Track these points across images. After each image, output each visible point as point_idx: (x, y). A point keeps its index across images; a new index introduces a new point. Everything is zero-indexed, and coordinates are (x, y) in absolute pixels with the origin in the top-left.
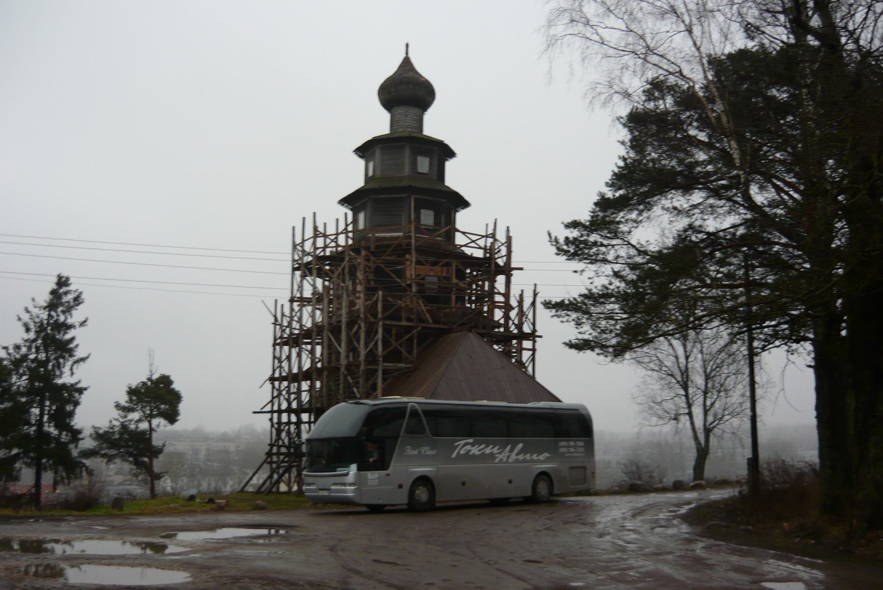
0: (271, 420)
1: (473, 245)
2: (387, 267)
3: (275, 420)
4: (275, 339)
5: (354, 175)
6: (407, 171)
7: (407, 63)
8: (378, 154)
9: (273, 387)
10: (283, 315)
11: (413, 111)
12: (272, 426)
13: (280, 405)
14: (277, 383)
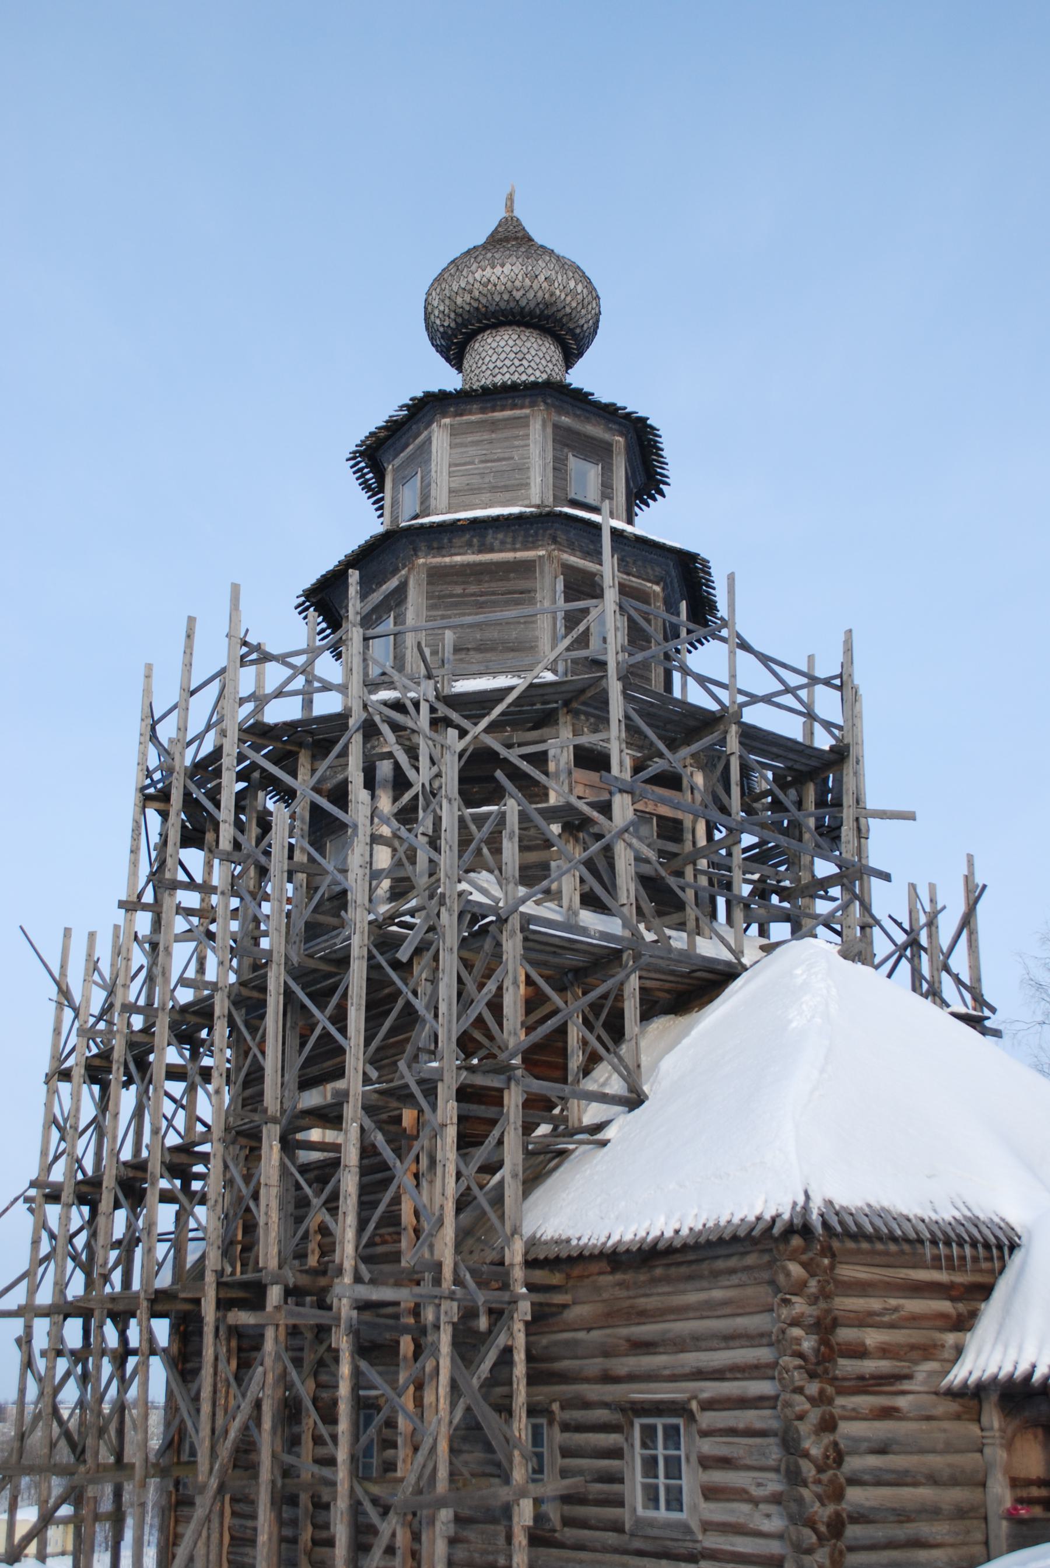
0: (25, 1342)
1: (788, 700)
2: (509, 746)
3: (40, 1341)
4: (58, 1057)
9: (42, 1224)
10: (93, 966)
12: (28, 1364)
13: (61, 1286)
14: (53, 1212)
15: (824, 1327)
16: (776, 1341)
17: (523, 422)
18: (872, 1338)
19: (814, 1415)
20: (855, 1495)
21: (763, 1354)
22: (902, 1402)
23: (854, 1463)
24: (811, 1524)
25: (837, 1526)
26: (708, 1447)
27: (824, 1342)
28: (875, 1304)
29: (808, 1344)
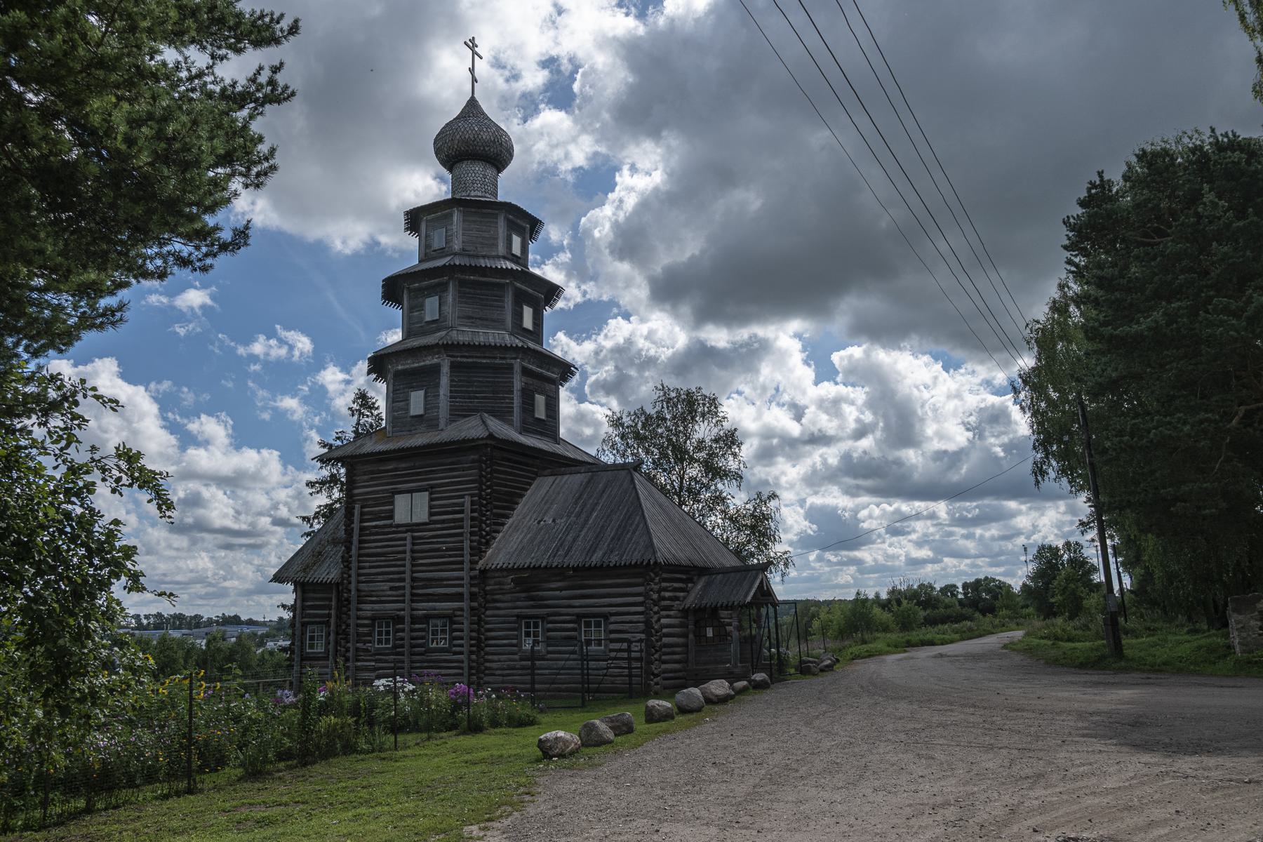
6: (501, 249)
7: (472, 104)
8: (456, 216)
11: (490, 172)
16: (646, 595)
17: (496, 217)
18: (667, 594)
19: (656, 617)
20: (665, 640)
22: (672, 613)
23: (665, 630)
26: (612, 627)
29: (655, 596)
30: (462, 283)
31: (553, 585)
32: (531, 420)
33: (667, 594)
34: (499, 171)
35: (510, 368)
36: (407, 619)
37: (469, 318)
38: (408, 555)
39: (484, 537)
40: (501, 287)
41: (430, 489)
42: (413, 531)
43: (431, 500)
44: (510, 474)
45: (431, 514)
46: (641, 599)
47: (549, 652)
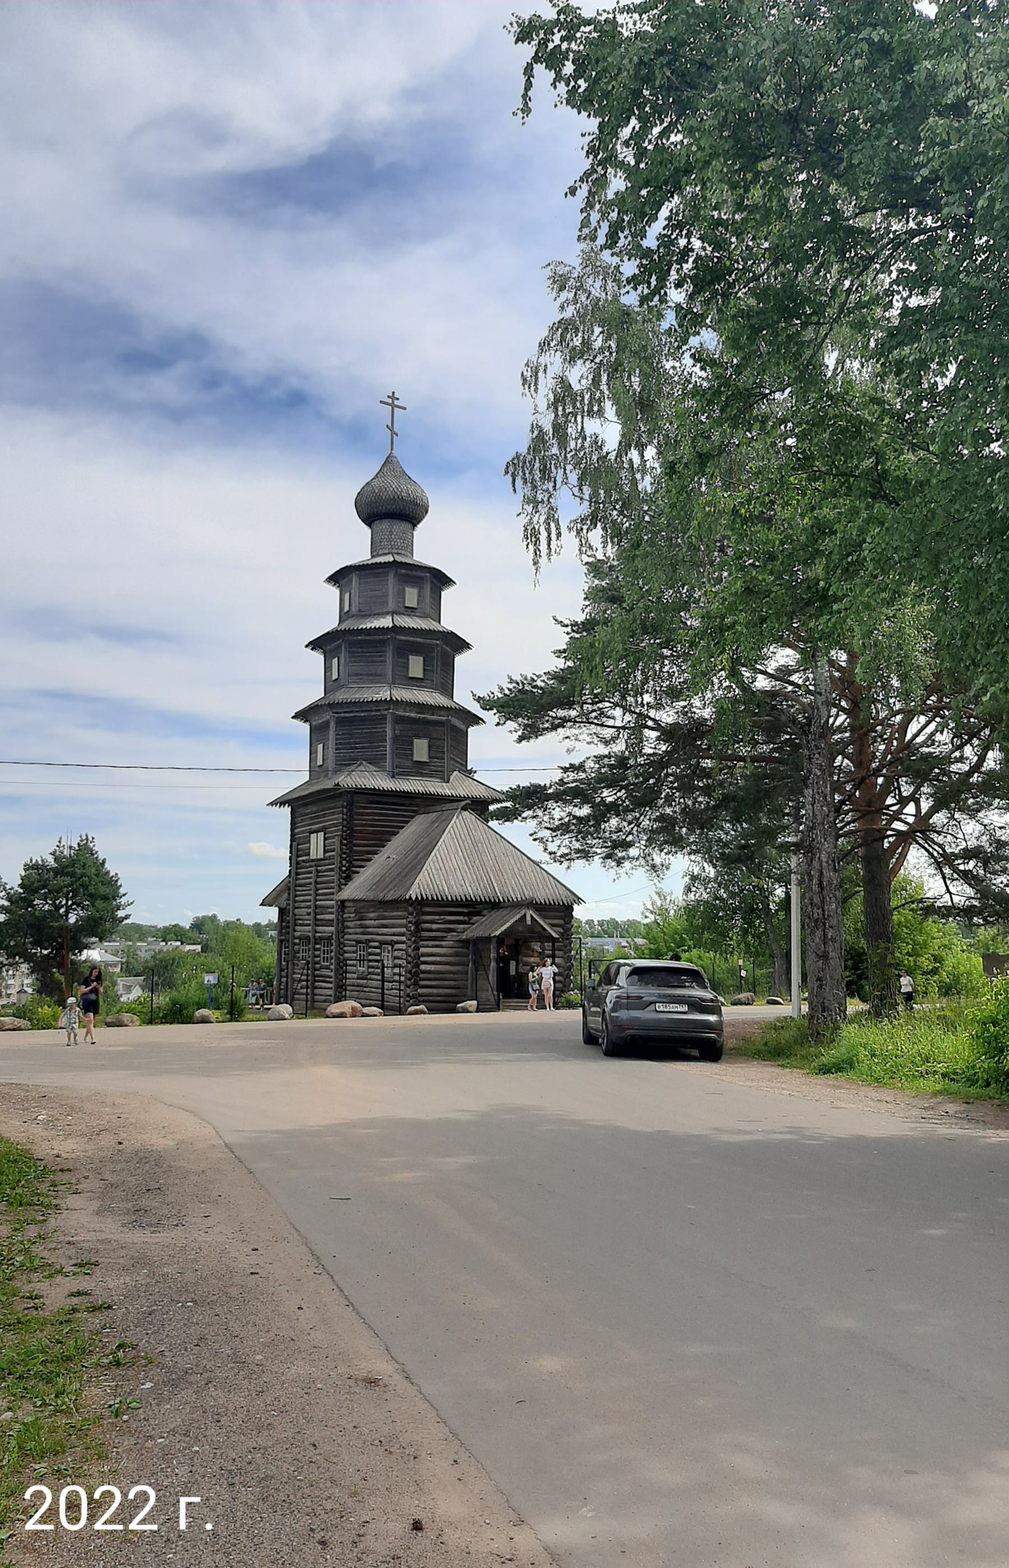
5: (326, 611)
15: (417, 924)
17: (387, 574)
18: (434, 926)
20: (423, 967)
21: (404, 930)
22: (443, 943)
24: (410, 972)
25: (416, 974)
26: (396, 953)
27: (417, 927)
28: (437, 917)
30: (352, 644)
31: (372, 915)
32: (408, 763)
33: (434, 926)
34: (414, 525)
35: (384, 718)
36: (312, 940)
37: (357, 675)
38: (312, 887)
39: (344, 872)
40: (383, 643)
41: (324, 829)
42: (316, 866)
43: (325, 839)
44: (380, 815)
45: (325, 852)
46: (404, 930)
47: (369, 973)
